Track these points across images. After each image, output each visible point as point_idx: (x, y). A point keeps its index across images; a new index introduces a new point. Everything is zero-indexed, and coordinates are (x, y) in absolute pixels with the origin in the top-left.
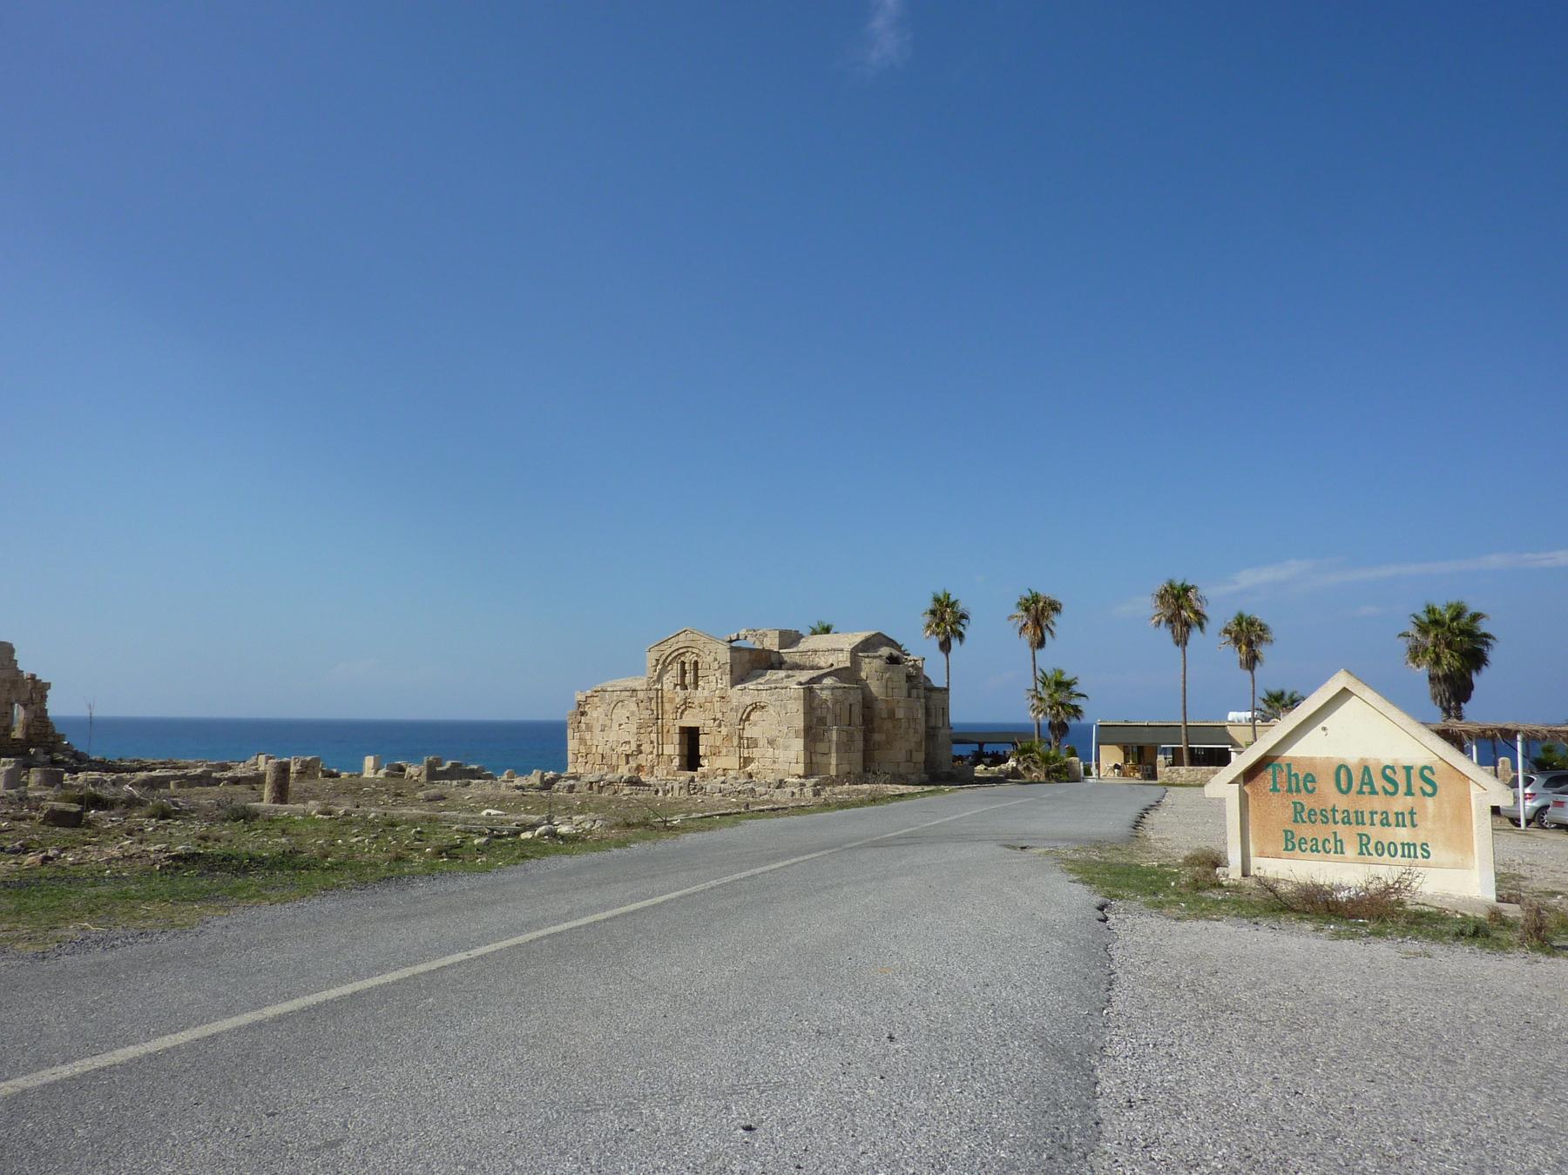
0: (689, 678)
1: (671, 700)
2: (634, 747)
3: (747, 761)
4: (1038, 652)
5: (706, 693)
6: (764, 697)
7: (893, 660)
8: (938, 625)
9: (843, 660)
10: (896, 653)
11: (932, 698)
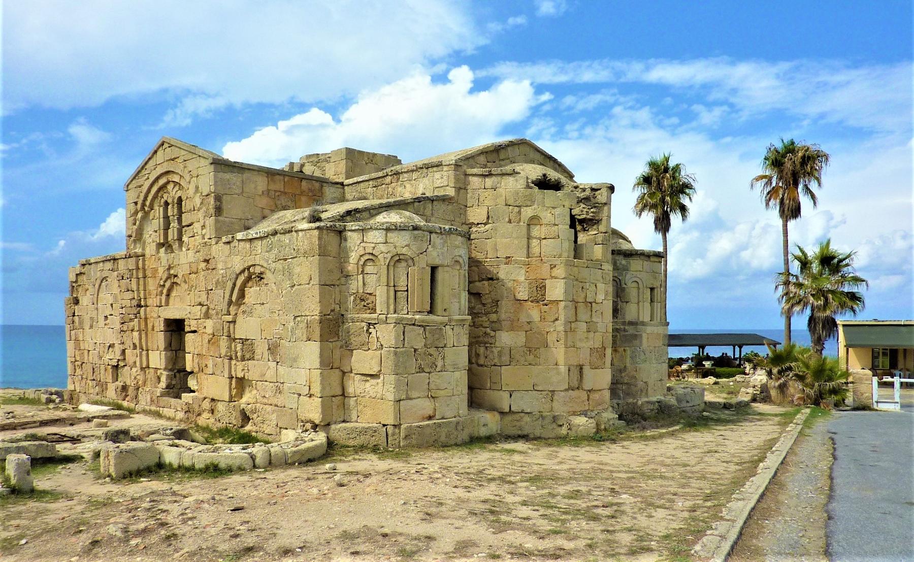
0: (172, 234)
3: (241, 384)
4: (792, 224)
6: (260, 255)
7: (544, 184)
8: (652, 195)
9: (440, 183)
10: (553, 175)
11: (633, 275)
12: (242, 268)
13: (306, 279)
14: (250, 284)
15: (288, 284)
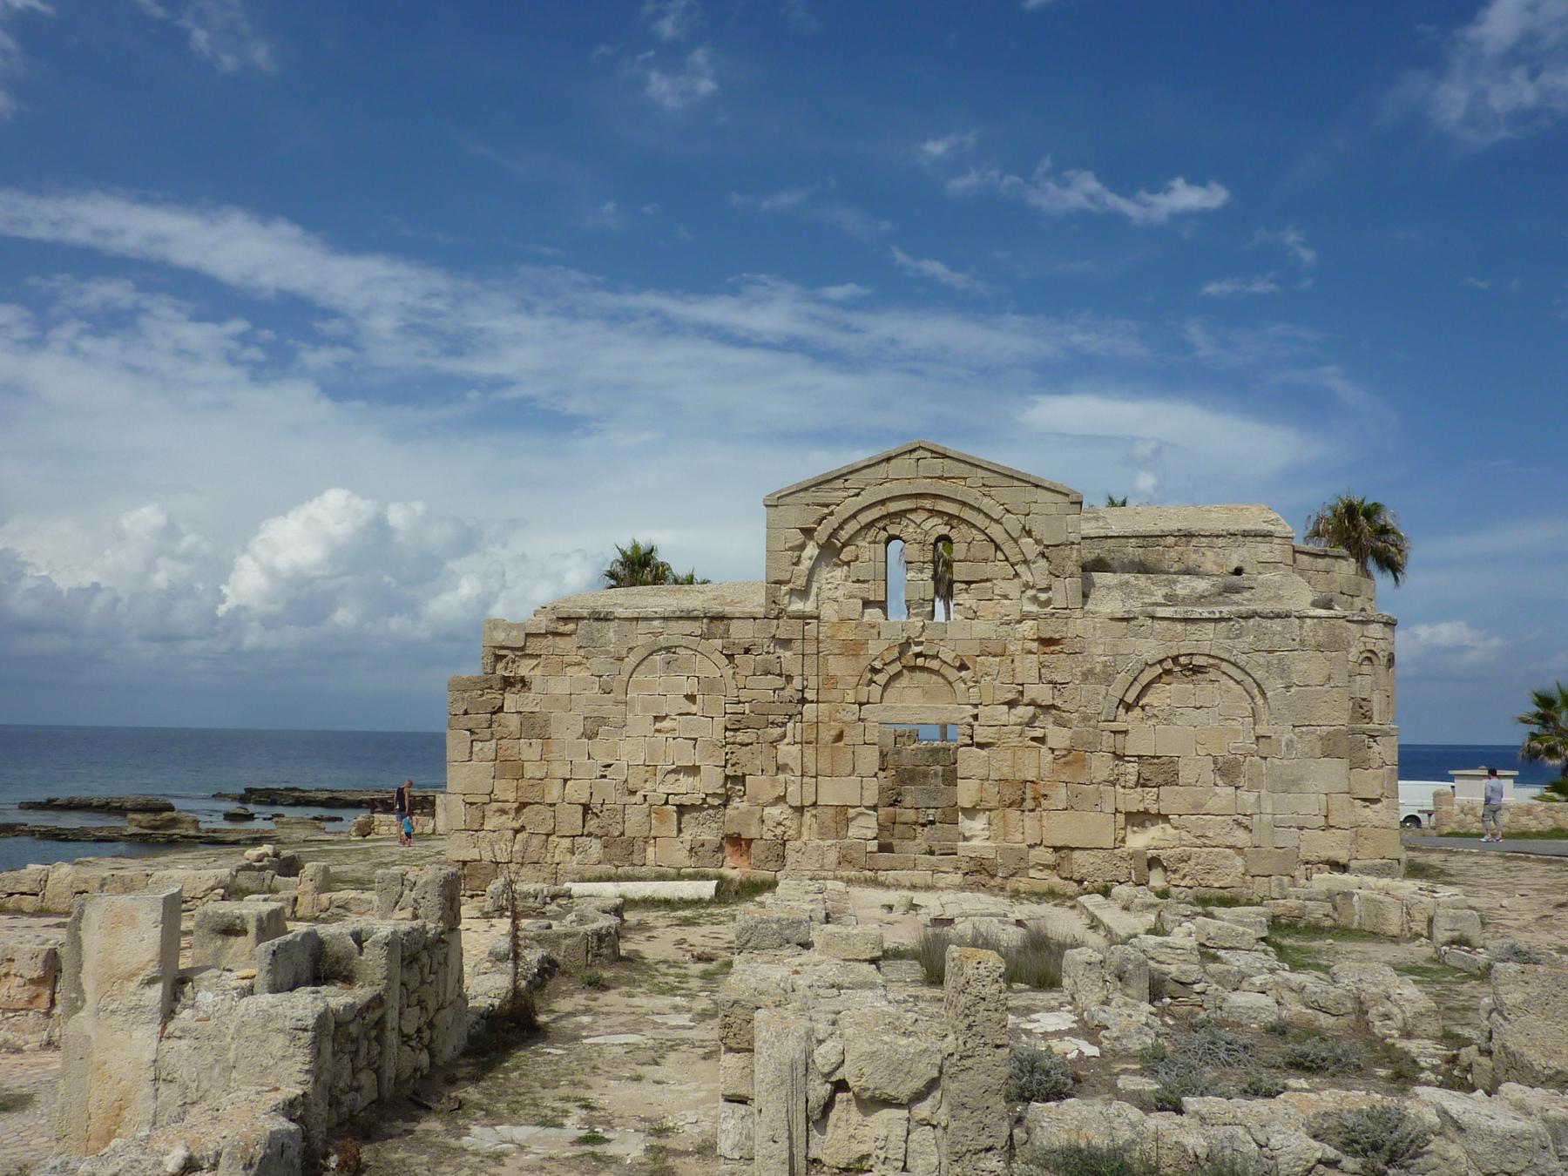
1: (853, 649)
2: (710, 780)
5: (982, 628)
12: (1161, 657)
13: (1320, 679)
14: (1166, 679)
15: (1279, 684)
